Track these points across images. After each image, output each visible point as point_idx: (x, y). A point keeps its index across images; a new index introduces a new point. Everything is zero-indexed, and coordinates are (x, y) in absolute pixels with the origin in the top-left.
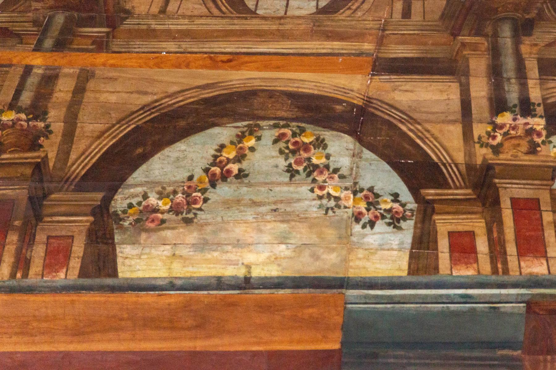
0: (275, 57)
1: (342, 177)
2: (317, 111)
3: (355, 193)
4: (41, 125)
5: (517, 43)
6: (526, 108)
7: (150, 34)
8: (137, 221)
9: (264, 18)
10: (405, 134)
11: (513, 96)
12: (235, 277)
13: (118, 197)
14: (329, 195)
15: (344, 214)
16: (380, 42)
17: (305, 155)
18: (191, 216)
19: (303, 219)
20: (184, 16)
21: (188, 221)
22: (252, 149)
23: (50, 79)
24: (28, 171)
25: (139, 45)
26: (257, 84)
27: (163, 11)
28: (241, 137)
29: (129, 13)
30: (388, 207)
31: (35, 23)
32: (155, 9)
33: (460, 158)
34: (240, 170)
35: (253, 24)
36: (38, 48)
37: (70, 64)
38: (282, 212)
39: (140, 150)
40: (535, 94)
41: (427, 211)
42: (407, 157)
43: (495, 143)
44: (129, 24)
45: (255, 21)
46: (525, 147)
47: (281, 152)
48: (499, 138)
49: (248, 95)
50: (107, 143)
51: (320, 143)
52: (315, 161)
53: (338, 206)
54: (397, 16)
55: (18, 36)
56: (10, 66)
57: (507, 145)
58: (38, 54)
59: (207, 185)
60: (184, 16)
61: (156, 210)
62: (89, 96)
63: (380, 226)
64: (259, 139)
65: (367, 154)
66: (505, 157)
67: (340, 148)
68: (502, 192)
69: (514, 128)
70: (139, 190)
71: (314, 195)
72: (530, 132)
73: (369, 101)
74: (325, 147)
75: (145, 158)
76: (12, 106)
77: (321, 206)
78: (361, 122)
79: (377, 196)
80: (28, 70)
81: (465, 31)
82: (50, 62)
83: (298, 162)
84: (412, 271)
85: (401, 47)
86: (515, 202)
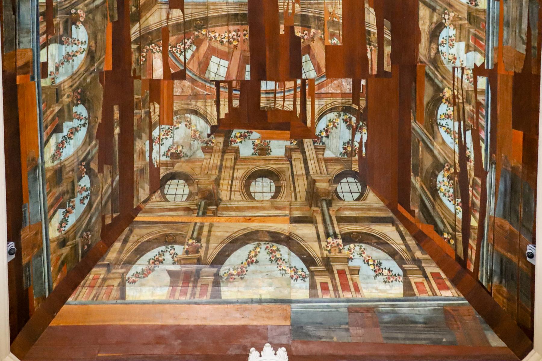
0: (262, 218)
1: (286, 262)
2: (276, 238)
3: (290, 268)
4: (199, 244)
5: (328, 210)
6: (335, 236)
7: (227, 209)
8: (227, 278)
9: (258, 201)
10: (302, 246)
11: (331, 232)
12: (257, 299)
13: (221, 270)
14: (283, 269)
15: (288, 276)
16: (290, 210)
17: (274, 254)
18: (243, 277)
19: (276, 278)
20: (236, 201)
21: (242, 279)
22: (259, 252)
23: (201, 228)
24: (196, 261)
25: (226, 213)
26: (258, 228)
27: (230, 199)
28: (256, 248)
29: (221, 200)
30: (300, 273)
31: (197, 205)
32: (228, 199)
33: (320, 255)
34: (256, 260)
35: (255, 204)
36: (198, 216)
37: (207, 222)
38: (269, 275)
39: (227, 253)
40: (337, 231)
41: (312, 274)
42: (304, 255)
43: (329, 249)
44: (222, 205)
45: (255, 203)
46: (337, 251)
47: (267, 253)
48: (330, 248)
49: (257, 232)
50: (218, 250)
51: (278, 250)
52: (278, 256)
53: (286, 273)
54: (294, 199)
55: (192, 210)
56: (190, 222)
57: (332, 250)
58: (198, 218)
59: (247, 266)
60: (236, 201)
61: (232, 275)
62: (212, 233)
63: (299, 279)
64: (261, 248)
65: (292, 254)
66: (332, 255)
67: (284, 251)
68: (333, 267)
69: (333, 243)
70: (228, 267)
71: (278, 269)
72: (338, 245)
73: (290, 233)
74: (280, 251)
75: (228, 256)
76: (192, 238)
77: (281, 273)
78: (289, 241)
79: (297, 269)
80: (196, 223)
81: (313, 205)
82: (201, 221)
83: (273, 257)
84: (311, 295)
85: (297, 212)
86: (338, 271)
